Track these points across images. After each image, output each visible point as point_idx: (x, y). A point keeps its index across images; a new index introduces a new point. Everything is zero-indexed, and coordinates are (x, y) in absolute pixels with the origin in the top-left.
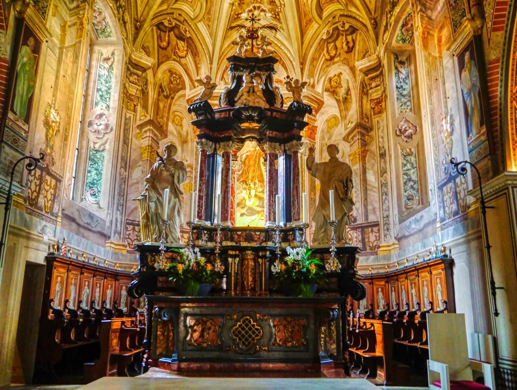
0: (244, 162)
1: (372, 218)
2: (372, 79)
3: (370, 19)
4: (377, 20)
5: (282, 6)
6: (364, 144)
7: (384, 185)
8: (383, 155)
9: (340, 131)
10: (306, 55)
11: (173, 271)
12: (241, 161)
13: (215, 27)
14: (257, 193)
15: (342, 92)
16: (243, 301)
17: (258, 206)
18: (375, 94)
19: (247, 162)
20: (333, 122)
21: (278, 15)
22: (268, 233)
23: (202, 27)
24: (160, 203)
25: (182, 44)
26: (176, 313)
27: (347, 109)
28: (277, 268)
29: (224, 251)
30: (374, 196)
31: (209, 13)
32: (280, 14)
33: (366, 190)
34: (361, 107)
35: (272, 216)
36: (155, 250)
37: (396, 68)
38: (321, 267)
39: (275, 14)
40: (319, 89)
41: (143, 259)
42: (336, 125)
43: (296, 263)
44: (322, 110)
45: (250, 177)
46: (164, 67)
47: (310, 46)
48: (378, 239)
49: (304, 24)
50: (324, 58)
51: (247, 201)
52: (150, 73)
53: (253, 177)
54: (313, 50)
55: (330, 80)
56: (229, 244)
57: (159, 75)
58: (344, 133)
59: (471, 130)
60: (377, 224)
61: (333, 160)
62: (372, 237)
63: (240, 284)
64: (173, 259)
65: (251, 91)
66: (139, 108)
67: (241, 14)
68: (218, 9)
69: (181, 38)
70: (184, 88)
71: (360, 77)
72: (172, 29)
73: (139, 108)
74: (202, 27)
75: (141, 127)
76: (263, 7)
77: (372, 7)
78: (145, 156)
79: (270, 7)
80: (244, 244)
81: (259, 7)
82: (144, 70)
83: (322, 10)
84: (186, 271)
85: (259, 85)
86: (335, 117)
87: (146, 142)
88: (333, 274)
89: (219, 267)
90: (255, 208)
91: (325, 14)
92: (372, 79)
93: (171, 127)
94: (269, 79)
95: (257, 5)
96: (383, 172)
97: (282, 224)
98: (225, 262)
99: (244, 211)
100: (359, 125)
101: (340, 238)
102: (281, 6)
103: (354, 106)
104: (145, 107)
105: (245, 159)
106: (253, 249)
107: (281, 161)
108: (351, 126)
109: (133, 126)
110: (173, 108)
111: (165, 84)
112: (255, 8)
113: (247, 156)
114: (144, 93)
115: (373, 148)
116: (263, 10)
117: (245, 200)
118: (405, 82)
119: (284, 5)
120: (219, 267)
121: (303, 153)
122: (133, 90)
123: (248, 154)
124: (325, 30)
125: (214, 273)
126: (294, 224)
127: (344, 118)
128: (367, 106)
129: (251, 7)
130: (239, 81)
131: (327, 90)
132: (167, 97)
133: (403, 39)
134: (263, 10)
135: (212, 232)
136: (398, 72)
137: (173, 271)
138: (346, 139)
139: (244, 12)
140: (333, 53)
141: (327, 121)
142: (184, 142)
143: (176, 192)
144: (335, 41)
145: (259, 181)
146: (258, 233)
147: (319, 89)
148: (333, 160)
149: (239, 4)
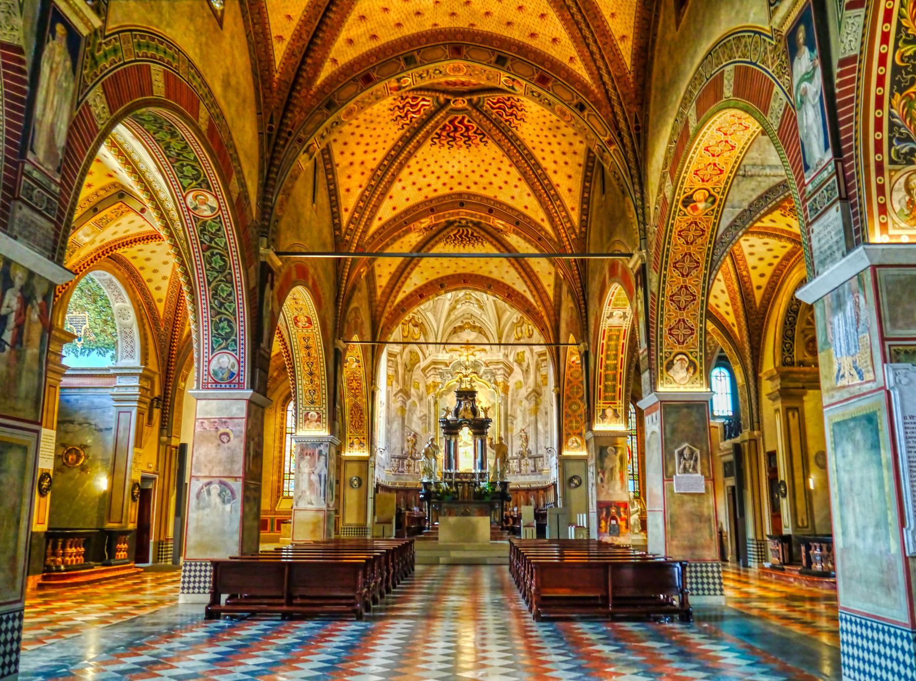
1: (540, 452)
2: (543, 361)
6: (537, 404)
7: (546, 432)
8: (546, 413)
9: (523, 392)
10: (503, 332)
11: (438, 492)
15: (525, 365)
16: (464, 502)
18: (544, 373)
20: (519, 385)
22: (474, 475)
23: (429, 314)
24: (430, 464)
25: (417, 330)
26: (440, 507)
27: (528, 378)
28: (477, 489)
29: (456, 483)
30: (541, 438)
31: (435, 307)
33: (537, 434)
34: (536, 378)
35: (475, 468)
36: (430, 483)
38: (493, 490)
40: (511, 359)
41: (425, 488)
42: (521, 387)
43: (484, 488)
44: (512, 375)
46: (407, 350)
47: (505, 325)
48: (543, 465)
49: (500, 312)
52: (399, 357)
54: (507, 329)
55: (518, 354)
56: (458, 480)
57: (404, 357)
58: (526, 394)
60: (542, 457)
61: (501, 444)
62: (540, 464)
63: (463, 496)
64: (436, 487)
65: (466, 409)
66: (394, 383)
69: (416, 325)
70: (419, 361)
71: (536, 357)
72: (410, 321)
73: (394, 383)
74: (429, 314)
75: (395, 395)
78: (399, 413)
80: (464, 480)
82: (395, 356)
84: (443, 491)
85: (469, 406)
86: (520, 382)
87: (399, 404)
88: (498, 492)
89: (454, 489)
92: (543, 361)
93: (413, 391)
94: (474, 401)
96: (547, 424)
97: (479, 471)
98: (456, 487)
100: (534, 391)
101: (502, 476)
103: (532, 377)
104: (397, 381)
106: (468, 483)
107: (479, 442)
108: (530, 390)
109: (392, 395)
110: (414, 377)
111: (408, 362)
114: (396, 371)
115: (542, 407)
120: (454, 489)
121: (488, 442)
122: (390, 373)
124: (515, 316)
125: (454, 492)
126: (484, 471)
127: (526, 383)
128: (539, 379)
130: (460, 405)
131: (516, 361)
132: (409, 371)
135: (450, 474)
137: (438, 492)
138: (526, 398)
140: (520, 335)
141: (516, 383)
142: (421, 399)
143: (436, 459)
144: (521, 326)
147: (511, 359)
148: (501, 444)
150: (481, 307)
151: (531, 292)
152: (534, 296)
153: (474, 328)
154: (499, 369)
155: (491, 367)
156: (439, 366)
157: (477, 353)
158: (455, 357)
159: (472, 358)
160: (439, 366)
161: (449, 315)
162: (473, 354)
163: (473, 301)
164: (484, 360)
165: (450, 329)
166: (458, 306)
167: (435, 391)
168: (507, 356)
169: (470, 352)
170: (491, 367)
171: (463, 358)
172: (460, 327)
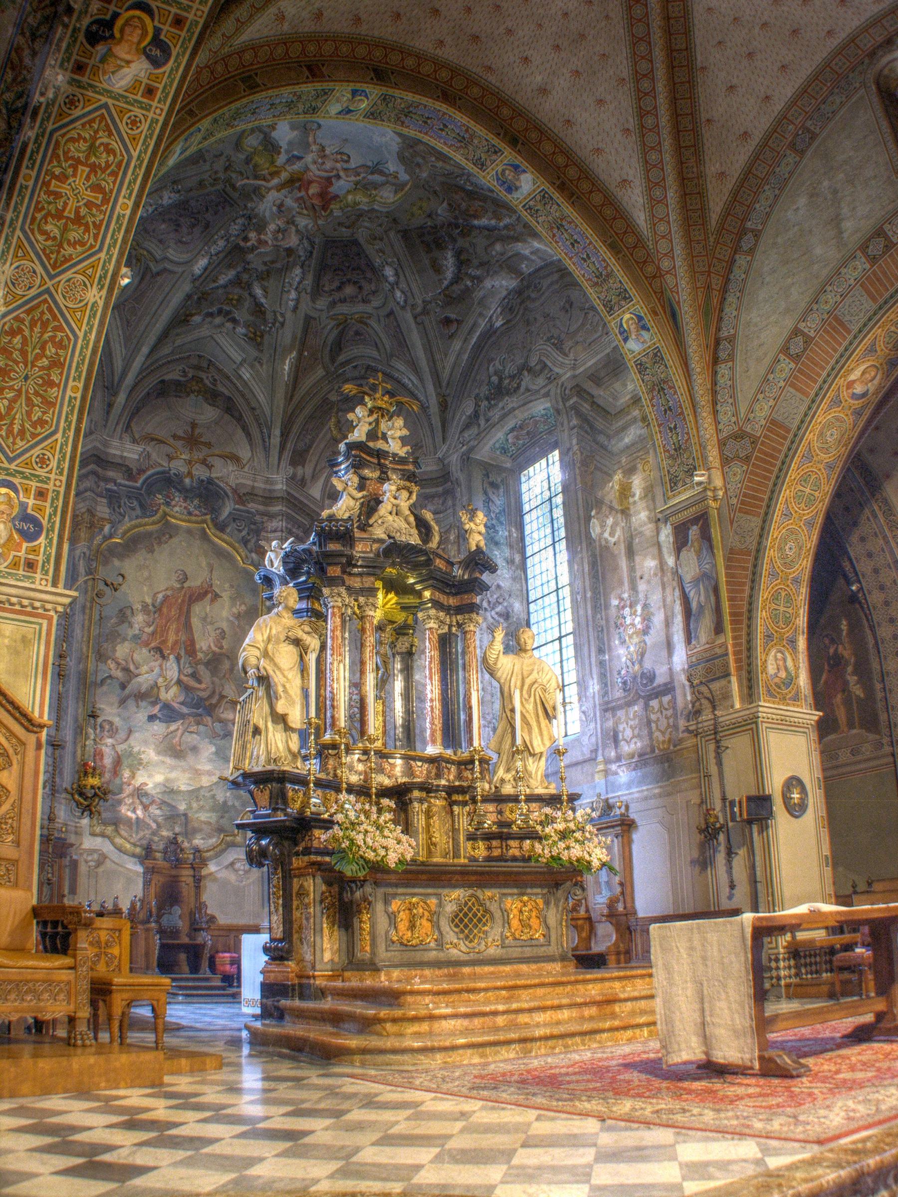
0: (160, 610)
3: (438, 394)
4: (449, 400)
5: (277, 324)
12: (154, 606)
13: (142, 328)
14: (183, 678)
17: (182, 703)
19: (165, 610)
21: (262, 337)
32: (266, 337)
37: (485, 493)
39: (255, 334)
45: (170, 644)
50: (329, 436)
51: (163, 690)
53: (176, 643)
59: (697, 638)
67: (192, 315)
68: (160, 299)
76: (236, 316)
77: (445, 375)
79: (252, 318)
81: (228, 313)
83: (341, 349)
90: (176, 705)
91: (342, 358)
95: (226, 308)
99: (156, 710)
102: (274, 324)
105: (162, 603)
112: (220, 311)
113: (166, 598)
116: (234, 321)
117: (158, 688)
118: (498, 519)
119: (282, 324)
123: (169, 593)
129: (214, 309)
133: (503, 448)
134: (234, 321)
136: (488, 501)
139: (199, 314)
145: (187, 652)
146: (419, 764)
149: (199, 299)
150: (255, 338)
151: (651, 185)
152: (653, 202)
153: (212, 396)
154: (271, 516)
155: (252, 506)
156: (111, 474)
157: (217, 462)
158: (154, 456)
159: (200, 472)
160: (111, 474)
161: (164, 336)
162: (204, 462)
163: (242, 315)
164: (232, 481)
165: (152, 382)
166: (197, 319)
167: (91, 539)
168: (303, 483)
169: (198, 455)
170: (252, 506)
171: (178, 466)
172: (177, 383)
